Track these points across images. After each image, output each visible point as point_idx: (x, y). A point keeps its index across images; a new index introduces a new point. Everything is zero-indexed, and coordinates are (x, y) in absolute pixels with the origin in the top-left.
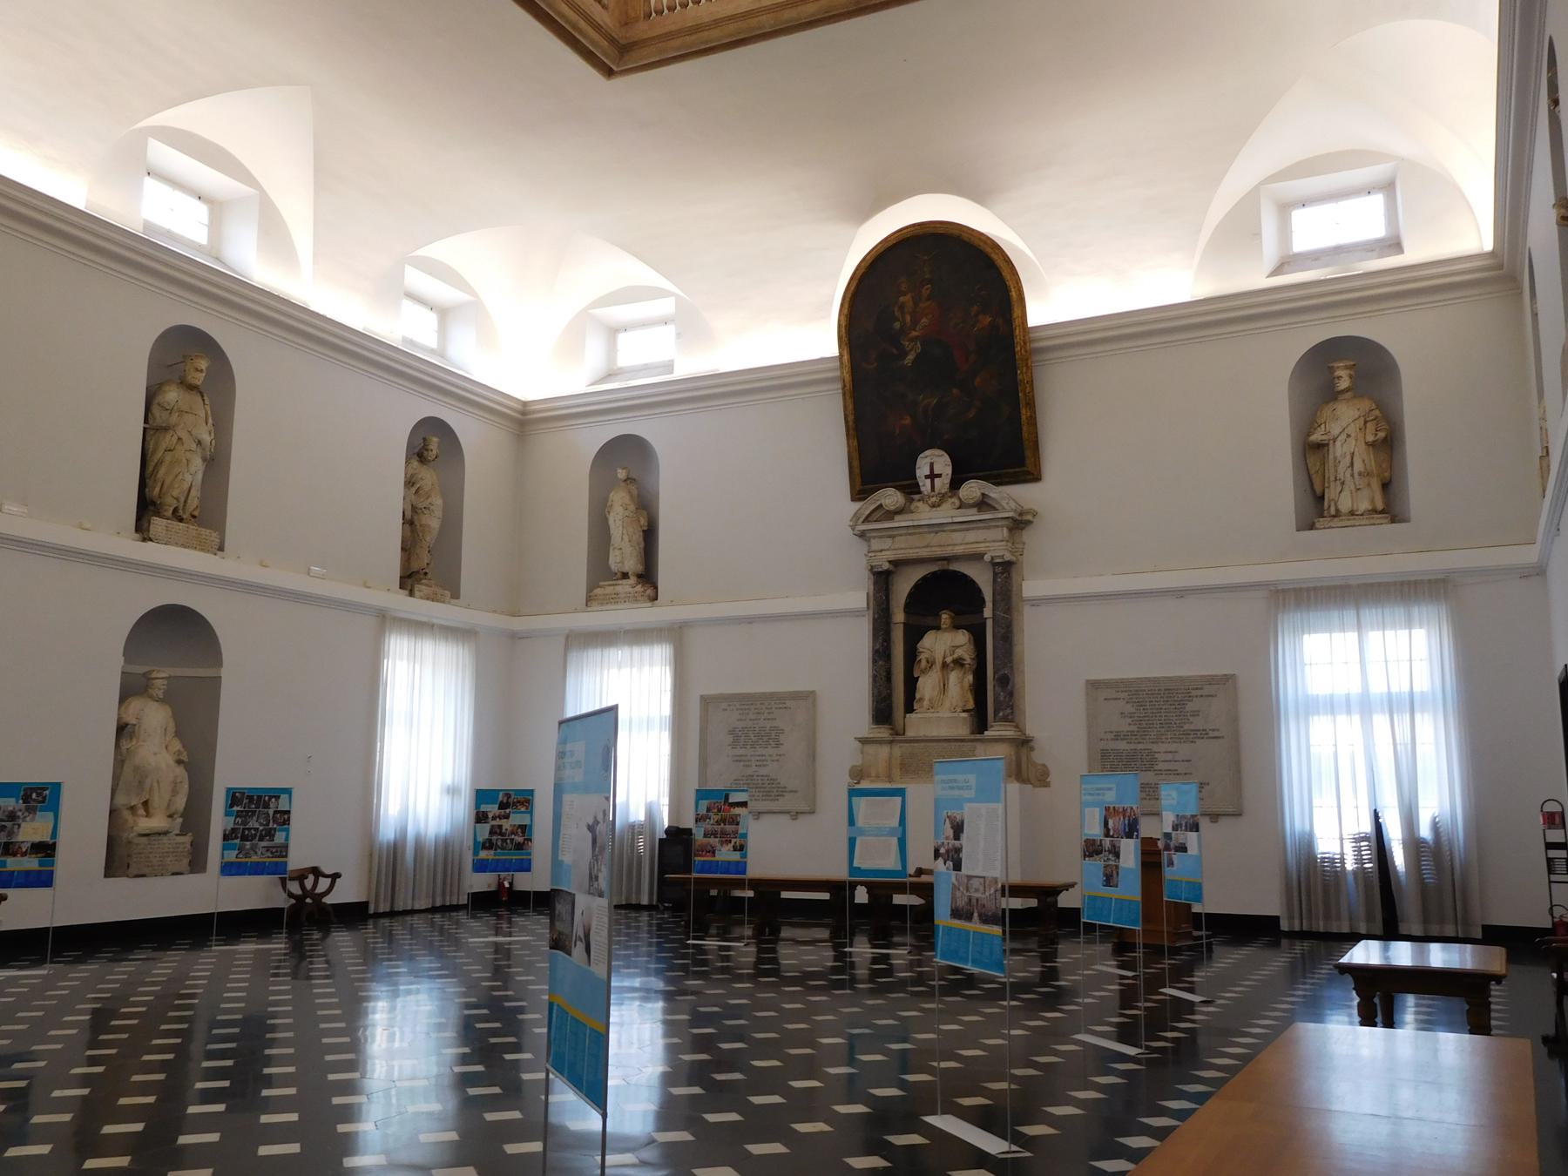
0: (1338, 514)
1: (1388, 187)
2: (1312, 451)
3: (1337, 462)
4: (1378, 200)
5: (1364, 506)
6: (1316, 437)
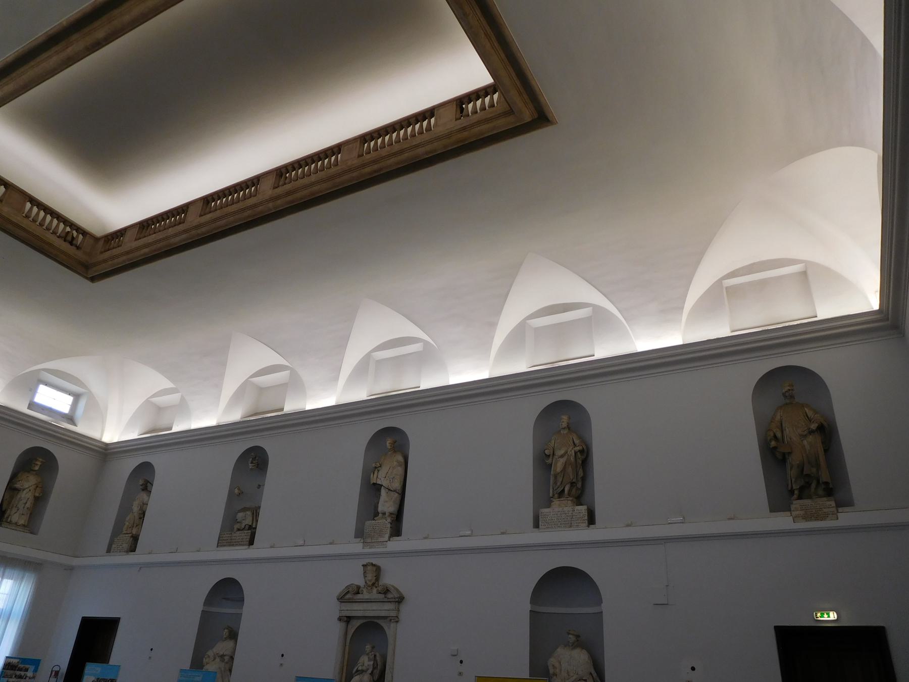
0: (10, 523)
1: (77, 397)
2: (12, 488)
3: (20, 499)
4: (70, 399)
5: (21, 522)
6: (18, 486)
